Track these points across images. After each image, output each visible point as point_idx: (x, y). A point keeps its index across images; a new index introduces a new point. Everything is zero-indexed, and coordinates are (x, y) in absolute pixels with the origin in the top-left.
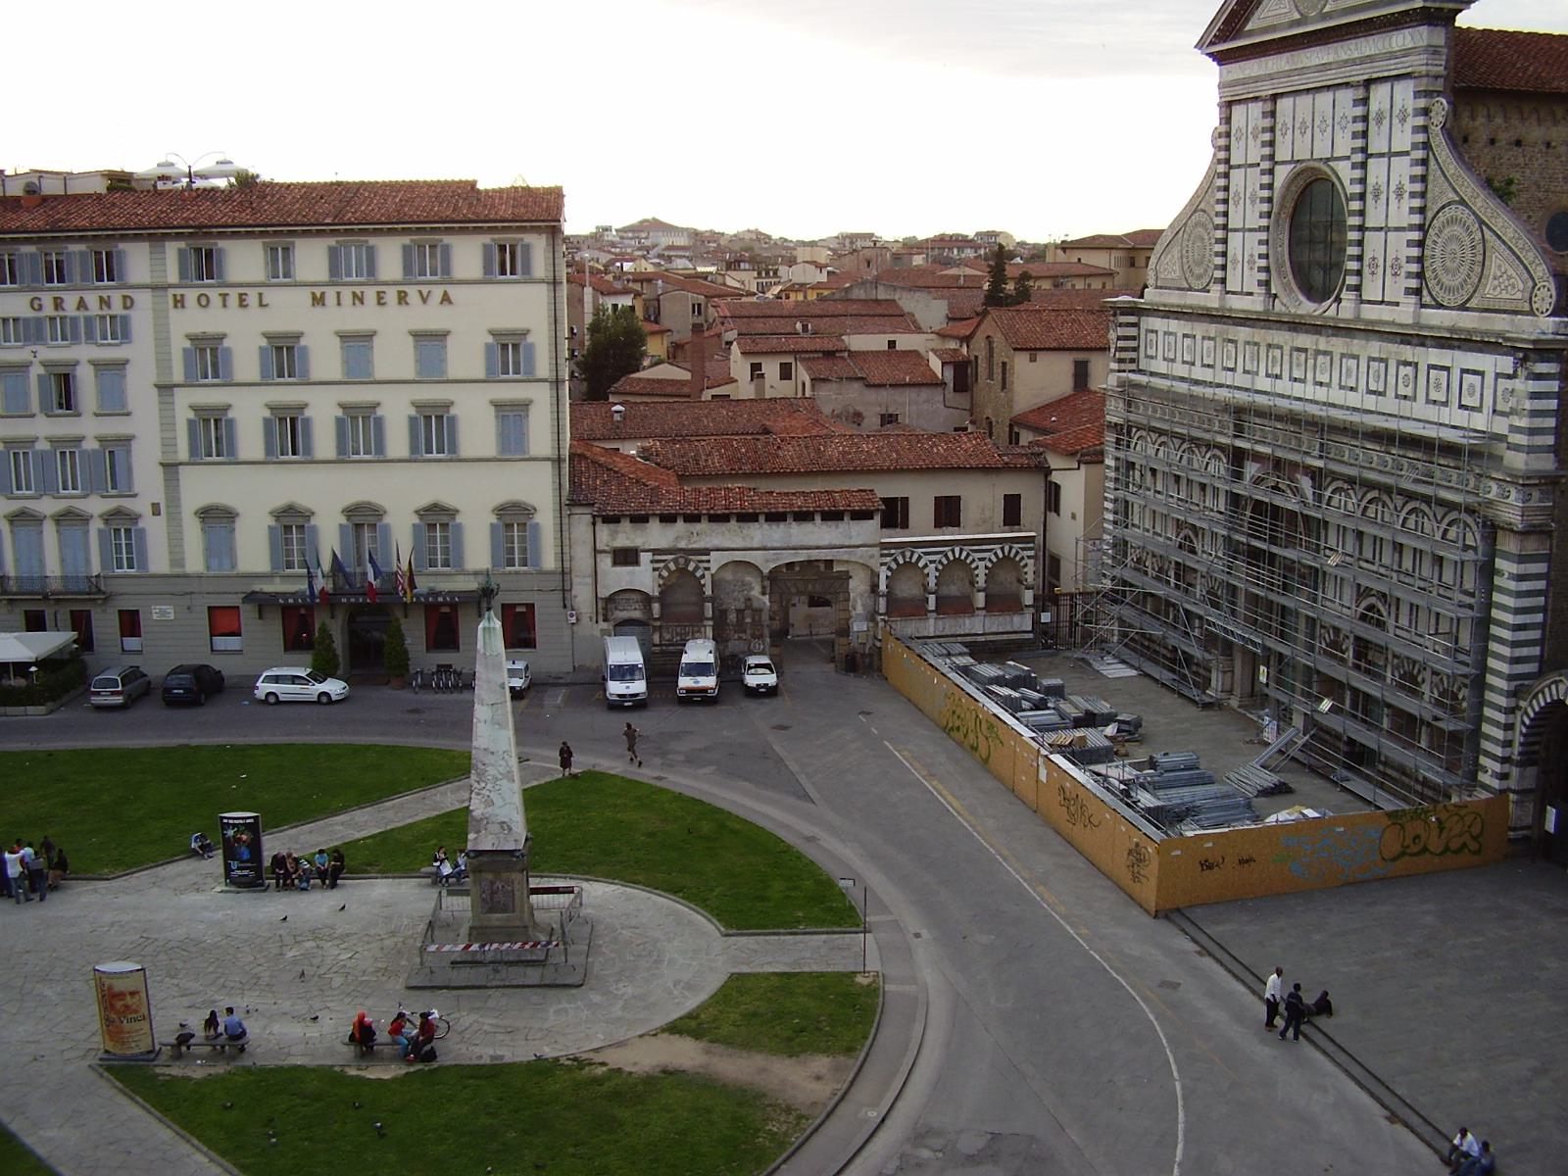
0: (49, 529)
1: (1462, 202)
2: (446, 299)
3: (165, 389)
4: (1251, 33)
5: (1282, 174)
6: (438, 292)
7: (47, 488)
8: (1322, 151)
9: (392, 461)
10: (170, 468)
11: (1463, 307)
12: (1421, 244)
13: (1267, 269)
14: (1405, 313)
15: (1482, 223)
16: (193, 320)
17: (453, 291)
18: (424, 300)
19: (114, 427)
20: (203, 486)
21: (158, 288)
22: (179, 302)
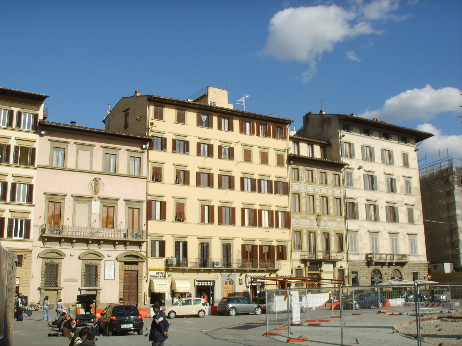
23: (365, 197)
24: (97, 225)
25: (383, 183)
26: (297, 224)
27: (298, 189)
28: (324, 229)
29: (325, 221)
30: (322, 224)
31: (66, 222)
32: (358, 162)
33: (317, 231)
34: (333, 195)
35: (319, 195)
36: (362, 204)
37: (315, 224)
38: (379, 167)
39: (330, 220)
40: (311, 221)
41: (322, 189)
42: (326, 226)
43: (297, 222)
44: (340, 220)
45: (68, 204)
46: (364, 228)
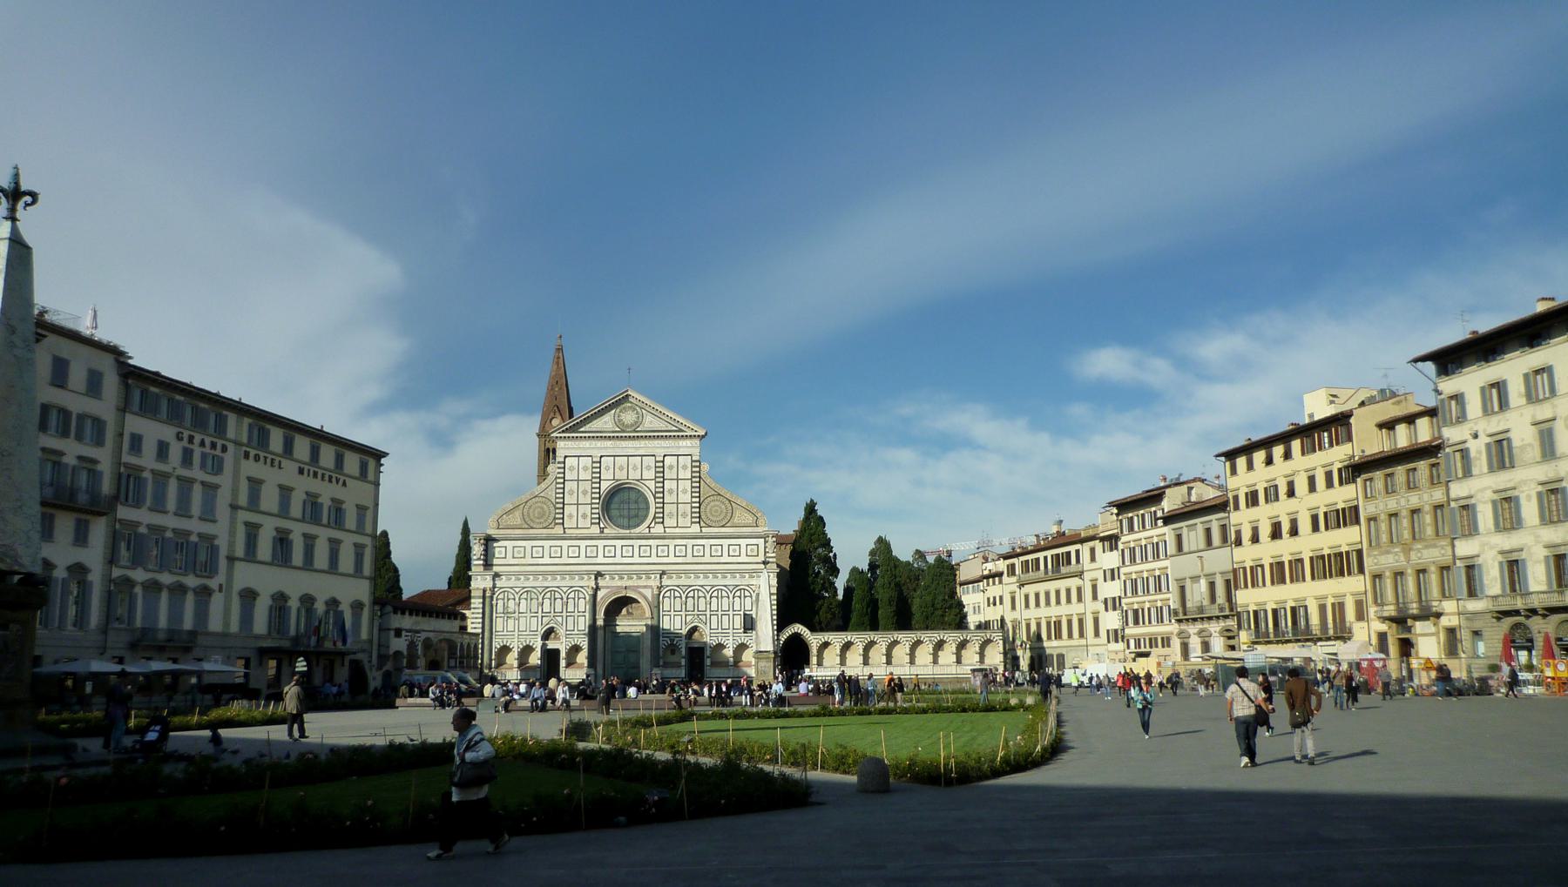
0: (164, 595)
1: (719, 495)
2: (344, 484)
3: (234, 507)
4: (585, 432)
5: (605, 486)
6: (342, 478)
7: (162, 567)
8: (634, 475)
9: (316, 571)
10: (231, 559)
11: (723, 526)
12: (699, 508)
13: (599, 518)
14: (695, 529)
15: (730, 501)
16: (250, 468)
17: (348, 480)
18: (337, 483)
19: (207, 528)
20: (245, 576)
21: (237, 443)
22: (247, 455)
23: (1490, 487)
24: (1206, 602)
25: (1530, 445)
26: (1376, 564)
27: (1375, 510)
28: (1417, 564)
29: (1419, 550)
30: (1413, 555)
31: (1189, 604)
32: (1476, 424)
33: (1406, 570)
34: (1431, 502)
35: (1406, 509)
36: (1485, 503)
37: (1402, 559)
38: (1522, 415)
39: (1426, 547)
40: (1396, 554)
41: (1410, 498)
42: (1420, 559)
43: (1376, 561)
44: (1444, 543)
45: (1188, 584)
46: (1492, 548)
